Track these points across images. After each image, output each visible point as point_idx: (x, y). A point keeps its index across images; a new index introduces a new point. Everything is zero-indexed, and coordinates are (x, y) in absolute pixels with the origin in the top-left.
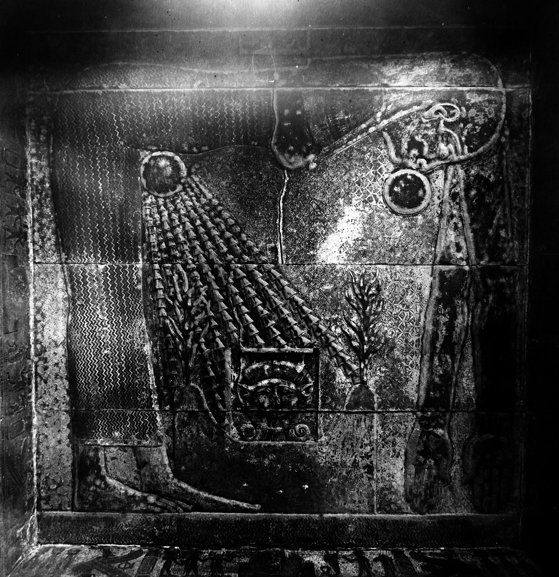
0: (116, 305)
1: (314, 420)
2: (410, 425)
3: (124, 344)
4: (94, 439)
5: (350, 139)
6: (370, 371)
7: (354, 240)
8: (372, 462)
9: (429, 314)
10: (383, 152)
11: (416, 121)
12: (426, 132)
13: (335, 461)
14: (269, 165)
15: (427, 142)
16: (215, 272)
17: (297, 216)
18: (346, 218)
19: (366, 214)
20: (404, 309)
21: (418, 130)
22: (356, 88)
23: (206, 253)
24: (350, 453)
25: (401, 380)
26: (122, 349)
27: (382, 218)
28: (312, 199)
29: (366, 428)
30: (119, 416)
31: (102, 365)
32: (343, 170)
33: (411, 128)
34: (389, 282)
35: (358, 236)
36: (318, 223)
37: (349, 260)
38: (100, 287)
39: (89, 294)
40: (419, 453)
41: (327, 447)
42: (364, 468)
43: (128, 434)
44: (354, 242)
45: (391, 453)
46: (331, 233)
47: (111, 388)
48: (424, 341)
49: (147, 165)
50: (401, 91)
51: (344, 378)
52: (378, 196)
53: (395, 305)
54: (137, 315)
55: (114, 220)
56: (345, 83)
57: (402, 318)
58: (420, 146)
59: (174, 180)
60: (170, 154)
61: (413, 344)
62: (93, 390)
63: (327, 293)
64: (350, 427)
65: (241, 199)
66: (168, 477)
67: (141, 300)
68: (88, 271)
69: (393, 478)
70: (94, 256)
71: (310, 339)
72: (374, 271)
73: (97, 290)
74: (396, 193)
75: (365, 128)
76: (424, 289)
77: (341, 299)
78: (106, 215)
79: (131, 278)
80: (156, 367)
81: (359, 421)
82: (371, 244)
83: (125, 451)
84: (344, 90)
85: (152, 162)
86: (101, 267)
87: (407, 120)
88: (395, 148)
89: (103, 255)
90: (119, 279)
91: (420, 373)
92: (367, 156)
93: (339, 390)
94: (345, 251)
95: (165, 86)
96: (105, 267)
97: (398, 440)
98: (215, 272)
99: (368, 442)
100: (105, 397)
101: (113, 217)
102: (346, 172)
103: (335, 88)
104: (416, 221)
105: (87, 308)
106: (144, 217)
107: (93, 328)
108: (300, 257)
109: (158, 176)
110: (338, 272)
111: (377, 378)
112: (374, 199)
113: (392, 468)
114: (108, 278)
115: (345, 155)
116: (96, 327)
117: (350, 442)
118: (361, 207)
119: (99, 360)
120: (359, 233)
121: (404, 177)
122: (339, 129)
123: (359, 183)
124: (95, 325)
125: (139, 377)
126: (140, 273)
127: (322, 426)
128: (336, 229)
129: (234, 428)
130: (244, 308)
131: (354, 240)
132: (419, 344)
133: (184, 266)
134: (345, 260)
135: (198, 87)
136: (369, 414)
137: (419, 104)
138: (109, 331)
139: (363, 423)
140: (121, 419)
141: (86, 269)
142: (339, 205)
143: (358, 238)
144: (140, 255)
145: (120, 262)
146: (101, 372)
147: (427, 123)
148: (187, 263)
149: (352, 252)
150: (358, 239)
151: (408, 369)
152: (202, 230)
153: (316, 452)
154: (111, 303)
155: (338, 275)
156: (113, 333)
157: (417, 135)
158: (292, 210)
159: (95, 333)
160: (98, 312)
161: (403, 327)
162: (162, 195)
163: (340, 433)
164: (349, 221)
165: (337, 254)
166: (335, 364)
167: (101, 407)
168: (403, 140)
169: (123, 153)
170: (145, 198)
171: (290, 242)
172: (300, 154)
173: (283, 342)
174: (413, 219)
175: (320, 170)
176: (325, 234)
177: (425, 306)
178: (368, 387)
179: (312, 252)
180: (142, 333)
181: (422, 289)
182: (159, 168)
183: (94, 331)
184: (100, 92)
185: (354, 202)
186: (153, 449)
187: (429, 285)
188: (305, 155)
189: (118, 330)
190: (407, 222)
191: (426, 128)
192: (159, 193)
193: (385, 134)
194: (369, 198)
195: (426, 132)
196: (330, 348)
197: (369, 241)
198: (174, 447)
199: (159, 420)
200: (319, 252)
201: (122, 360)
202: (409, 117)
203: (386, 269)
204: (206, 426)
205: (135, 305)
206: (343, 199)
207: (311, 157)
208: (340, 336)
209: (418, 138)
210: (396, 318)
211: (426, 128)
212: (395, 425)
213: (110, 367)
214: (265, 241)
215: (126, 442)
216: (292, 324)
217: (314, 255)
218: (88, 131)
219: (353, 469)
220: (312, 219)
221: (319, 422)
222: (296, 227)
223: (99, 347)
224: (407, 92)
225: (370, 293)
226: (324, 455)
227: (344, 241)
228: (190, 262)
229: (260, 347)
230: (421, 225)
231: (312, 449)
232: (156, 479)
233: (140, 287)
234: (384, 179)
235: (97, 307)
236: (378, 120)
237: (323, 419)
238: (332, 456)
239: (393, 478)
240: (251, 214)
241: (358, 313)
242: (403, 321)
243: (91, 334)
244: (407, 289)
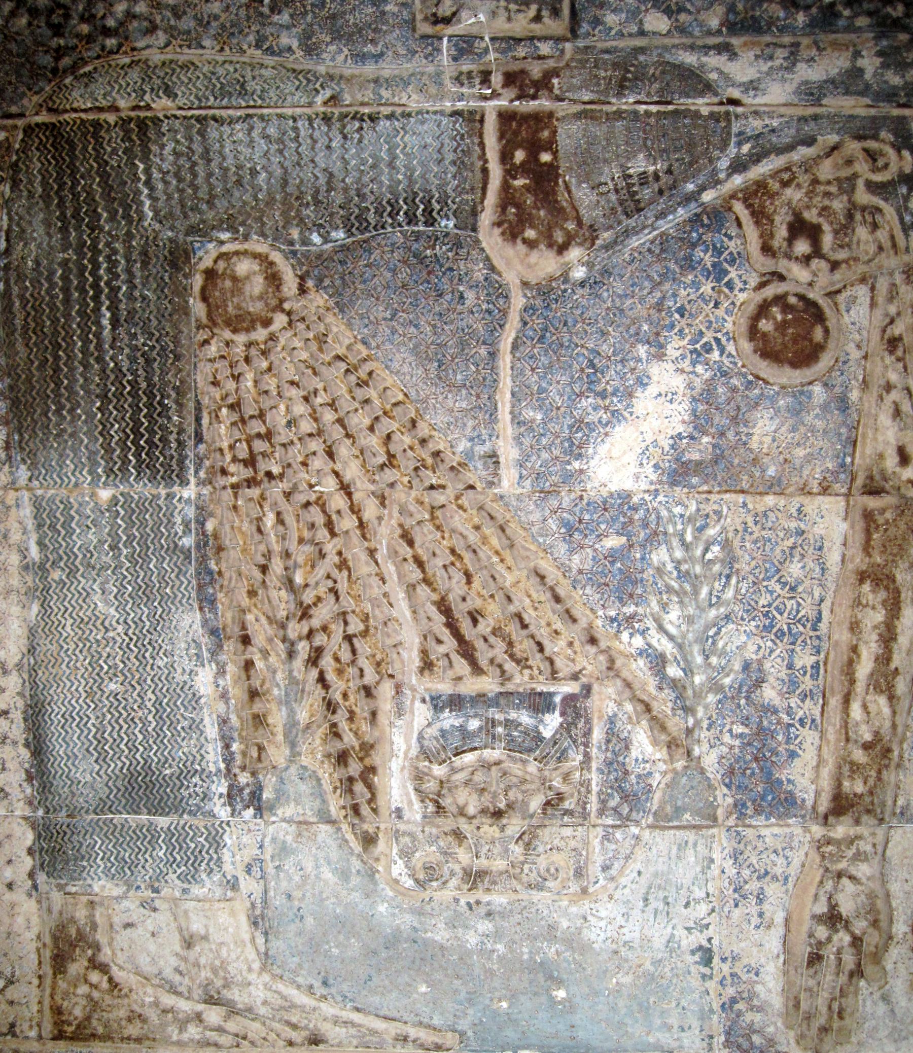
0: (136, 582)
1: (580, 846)
2: (797, 858)
3: (152, 669)
4: (85, 879)
5: (662, 215)
6: (708, 734)
7: (672, 437)
8: (710, 940)
9: (840, 605)
10: (733, 246)
11: (804, 179)
12: (826, 202)
13: (627, 938)
14: (480, 270)
15: (831, 223)
16: (355, 510)
17: (544, 385)
18: (652, 390)
19: (699, 380)
20: (785, 593)
21: (811, 198)
22: (670, 108)
23: (338, 467)
24: (661, 918)
25: (777, 754)
26: (149, 682)
27: (734, 390)
28: (577, 346)
29: (697, 863)
30: (141, 831)
31: (104, 715)
32: (646, 284)
33: (794, 195)
34: (751, 533)
35: (680, 428)
36: (590, 400)
37: (660, 482)
38: (101, 542)
39: (77, 556)
40: (819, 919)
41: (609, 906)
42: (693, 952)
43: (161, 871)
44: (671, 442)
45: (755, 920)
46: (619, 421)
47: (122, 768)
48: (829, 669)
49: (210, 274)
50: (771, 115)
51: (649, 749)
52: (724, 340)
53: (765, 583)
54: (182, 605)
55: (134, 394)
56: (648, 94)
57: (781, 614)
58: (813, 233)
59: (267, 305)
60: (261, 247)
61: (805, 673)
62: (84, 771)
63: (612, 556)
64: (661, 859)
65: (416, 347)
66: (250, 970)
67: (192, 570)
68: (76, 506)
69: (757, 974)
70: (90, 473)
71: (573, 661)
72: (716, 507)
73: (95, 548)
74: (764, 335)
75: (693, 192)
76: (830, 549)
77: (643, 571)
78: (118, 381)
79: (169, 521)
80: (225, 722)
81: (682, 846)
82: (710, 447)
83: (155, 910)
84: (646, 112)
85: (221, 265)
86: (105, 495)
87: (786, 176)
88: (761, 236)
89: (109, 472)
90: (143, 524)
91: (821, 738)
92: (699, 253)
93: (639, 776)
94: (652, 463)
95: (252, 103)
96: (114, 497)
97: (773, 890)
98: (355, 510)
99: (704, 895)
100: (109, 788)
101: (133, 387)
102: (653, 288)
103: (624, 107)
104: (810, 397)
105: (72, 588)
106: (200, 384)
107: (84, 632)
108: (551, 475)
109: (233, 296)
110: (635, 509)
111: (725, 750)
112: (715, 347)
113: (755, 953)
114: (119, 522)
115: (649, 250)
116: (91, 631)
117: (661, 894)
118: (686, 365)
119: (97, 706)
120: (684, 422)
121: (780, 299)
122: (636, 193)
123: (681, 311)
124: (90, 626)
125: (184, 744)
126: (191, 512)
127: (598, 859)
128: (631, 414)
129: (400, 862)
130: (423, 591)
131: (672, 437)
132: (818, 673)
133: (288, 495)
134: (652, 483)
135: (325, 103)
136: (704, 831)
137: (810, 141)
138: (119, 640)
139: (692, 851)
140: (146, 837)
141: (72, 500)
142: (639, 360)
143: (680, 434)
144: (192, 471)
145: (145, 485)
146: (101, 730)
147: (829, 183)
148: (295, 487)
149: (667, 465)
150: (680, 436)
151: (793, 730)
152: (329, 416)
153: (585, 918)
154: (125, 577)
155: (636, 517)
156: (128, 644)
157: (808, 207)
158: (533, 370)
159: (88, 644)
160: (97, 598)
161: (783, 634)
162: (241, 339)
163: (639, 873)
164: (660, 395)
165: (633, 469)
166: (630, 718)
167: (102, 811)
168: (777, 219)
169: (157, 246)
170: (206, 342)
171: (527, 441)
172: (550, 246)
173: (510, 666)
174: (802, 393)
175: (595, 283)
176: (607, 425)
177: (832, 587)
178: (702, 771)
179: (576, 465)
180: (193, 645)
181: (825, 549)
182: (235, 279)
183: (87, 639)
184: (111, 118)
185: (672, 351)
186: (217, 905)
187: (839, 540)
188: (562, 249)
189: (138, 638)
190: (790, 399)
191: (827, 194)
192: (235, 331)
193: (739, 208)
194: (705, 344)
195: (826, 202)
196: (619, 682)
197: (705, 439)
198: (265, 901)
199: (229, 842)
200: (592, 463)
201: (149, 705)
202: (788, 169)
203: (745, 505)
204: (334, 854)
205: (178, 583)
206: (646, 347)
207: (575, 253)
208: (641, 654)
209: (811, 216)
210: (766, 615)
211: (827, 194)
212: (764, 856)
213: (121, 721)
214: (471, 439)
215: (156, 891)
216: (532, 627)
217: (582, 471)
218: (84, 201)
219: (667, 955)
220: (577, 391)
221: (591, 850)
222: (541, 407)
223: (98, 674)
224: (782, 116)
225: (709, 556)
226: (602, 924)
227: (649, 438)
228: (304, 486)
229: (460, 679)
230: (820, 406)
231: (574, 909)
232: (222, 974)
233: (188, 541)
234: (738, 304)
235: (94, 587)
236: (722, 176)
237: (602, 843)
238: (621, 927)
239: (757, 974)
240: (440, 378)
241: (681, 602)
242: (782, 622)
243: (81, 645)
244: (793, 548)
